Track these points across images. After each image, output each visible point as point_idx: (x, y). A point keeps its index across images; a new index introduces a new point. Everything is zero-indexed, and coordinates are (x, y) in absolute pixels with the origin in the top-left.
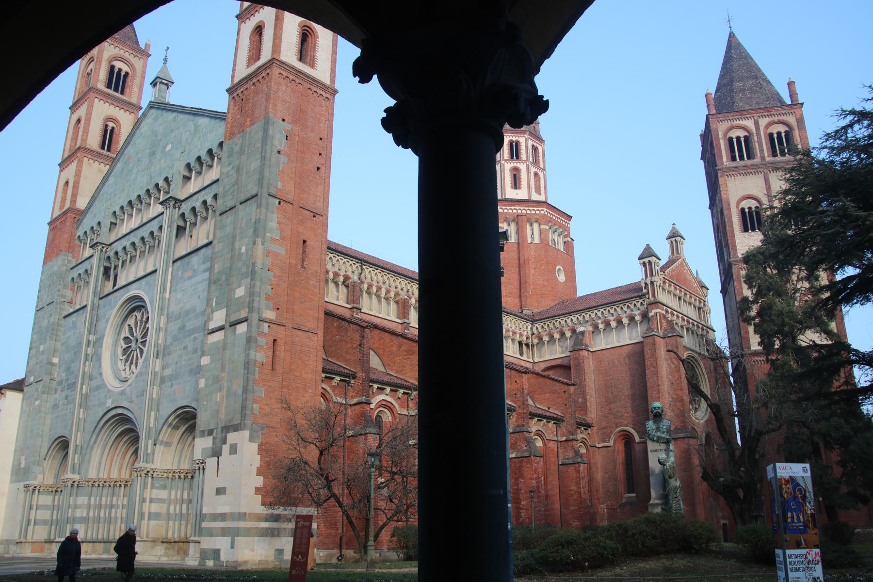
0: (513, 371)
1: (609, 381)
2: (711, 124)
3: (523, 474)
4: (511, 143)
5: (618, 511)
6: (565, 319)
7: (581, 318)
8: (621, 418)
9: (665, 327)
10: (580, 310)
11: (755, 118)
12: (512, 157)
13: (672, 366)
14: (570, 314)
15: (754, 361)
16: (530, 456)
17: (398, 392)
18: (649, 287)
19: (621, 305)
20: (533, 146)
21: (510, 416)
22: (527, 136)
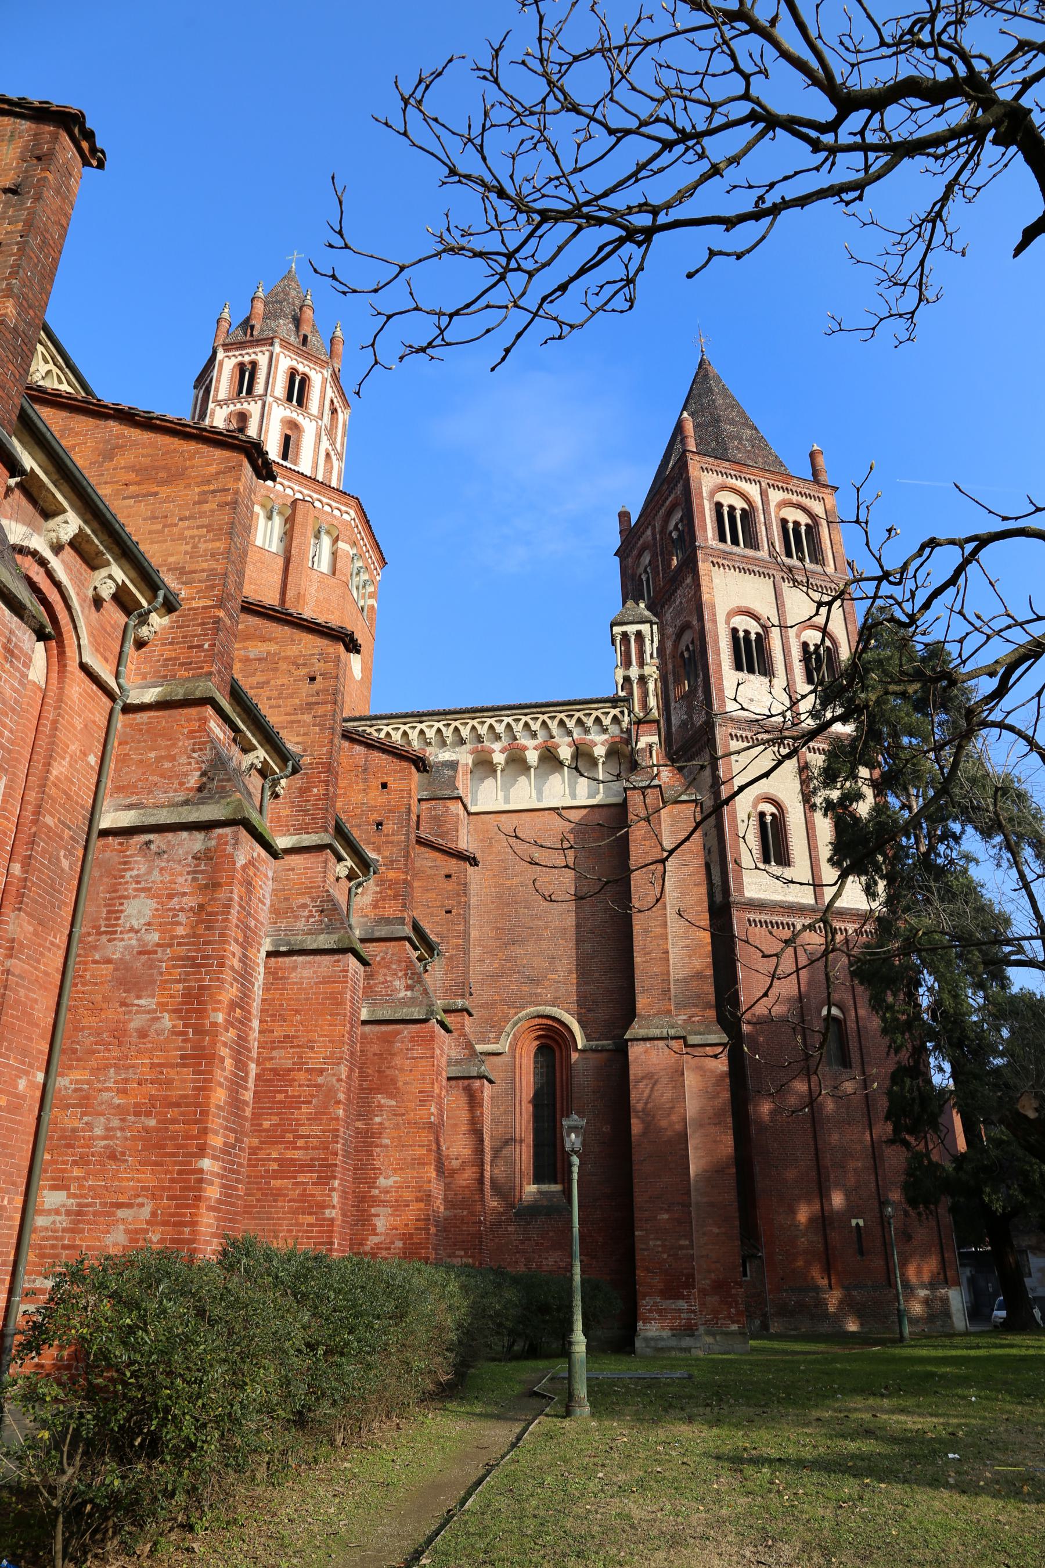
0: (376, 754)
1: (509, 888)
2: (690, 468)
3: (394, 1081)
4: (293, 373)
5: (511, 1229)
6: (403, 727)
7: (448, 732)
8: (537, 982)
9: (667, 780)
10: (446, 713)
11: (763, 484)
12: (289, 399)
13: (685, 869)
14: (420, 716)
15: (749, 920)
16: (425, 1021)
17: (103, 572)
18: (635, 686)
19: (562, 716)
20: (332, 401)
21: (359, 885)
22: (327, 373)
